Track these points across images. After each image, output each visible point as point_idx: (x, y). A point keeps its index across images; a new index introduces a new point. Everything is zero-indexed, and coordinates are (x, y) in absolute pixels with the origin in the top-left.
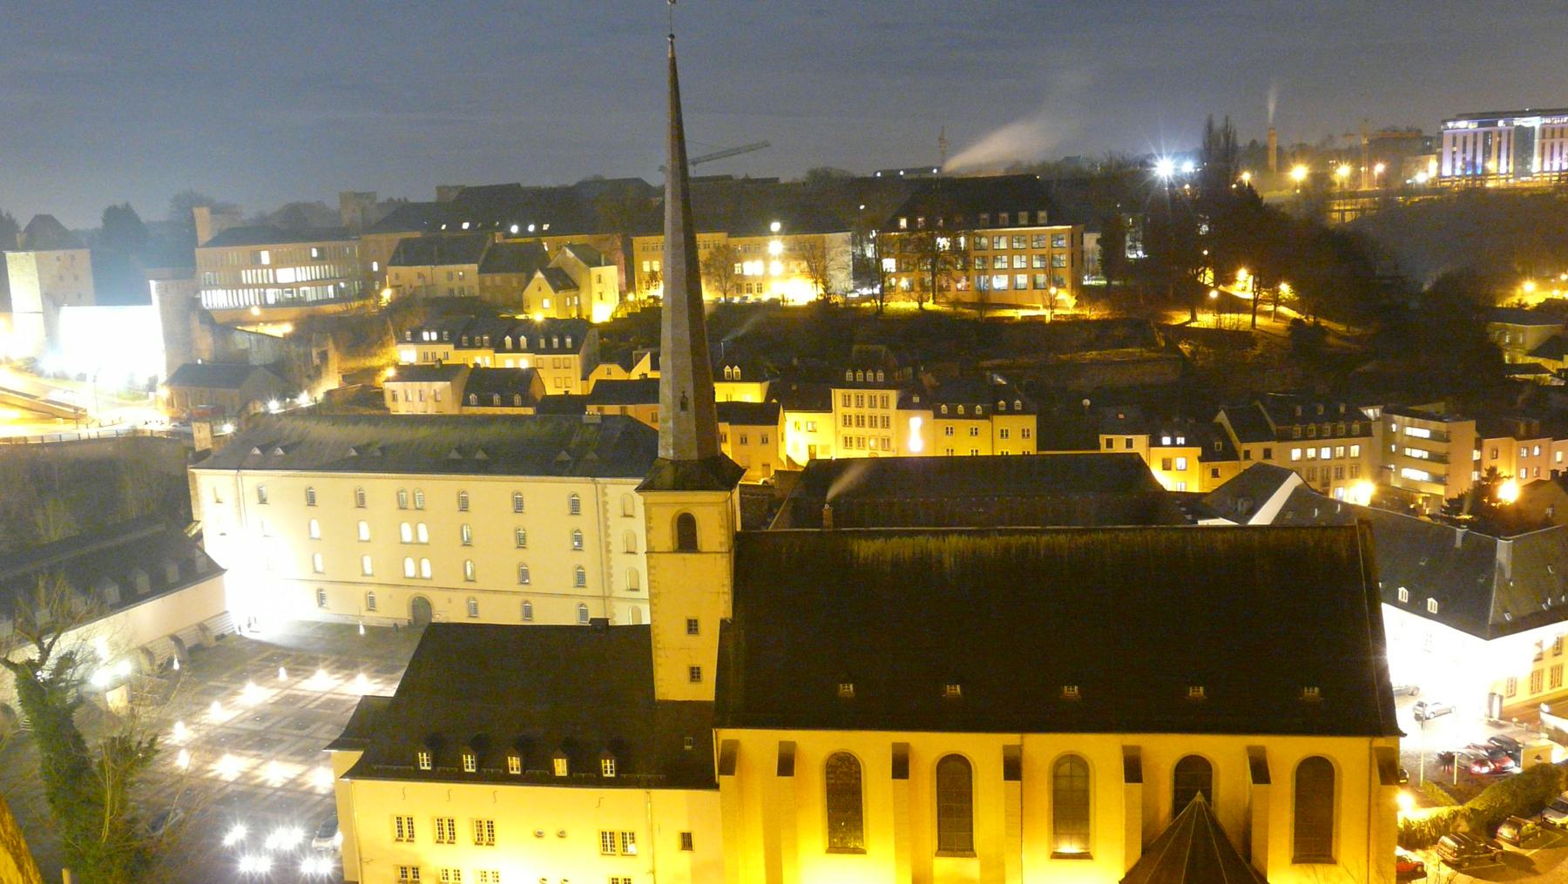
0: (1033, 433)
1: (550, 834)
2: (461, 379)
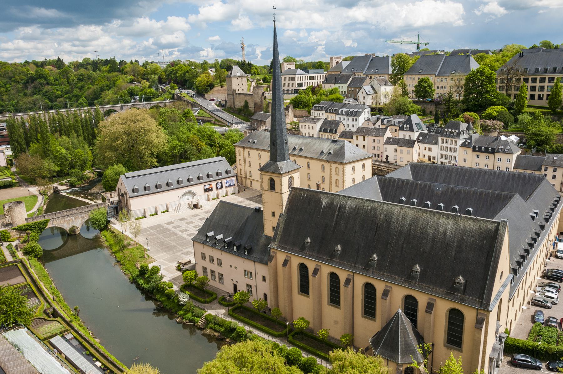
2: (319, 124)
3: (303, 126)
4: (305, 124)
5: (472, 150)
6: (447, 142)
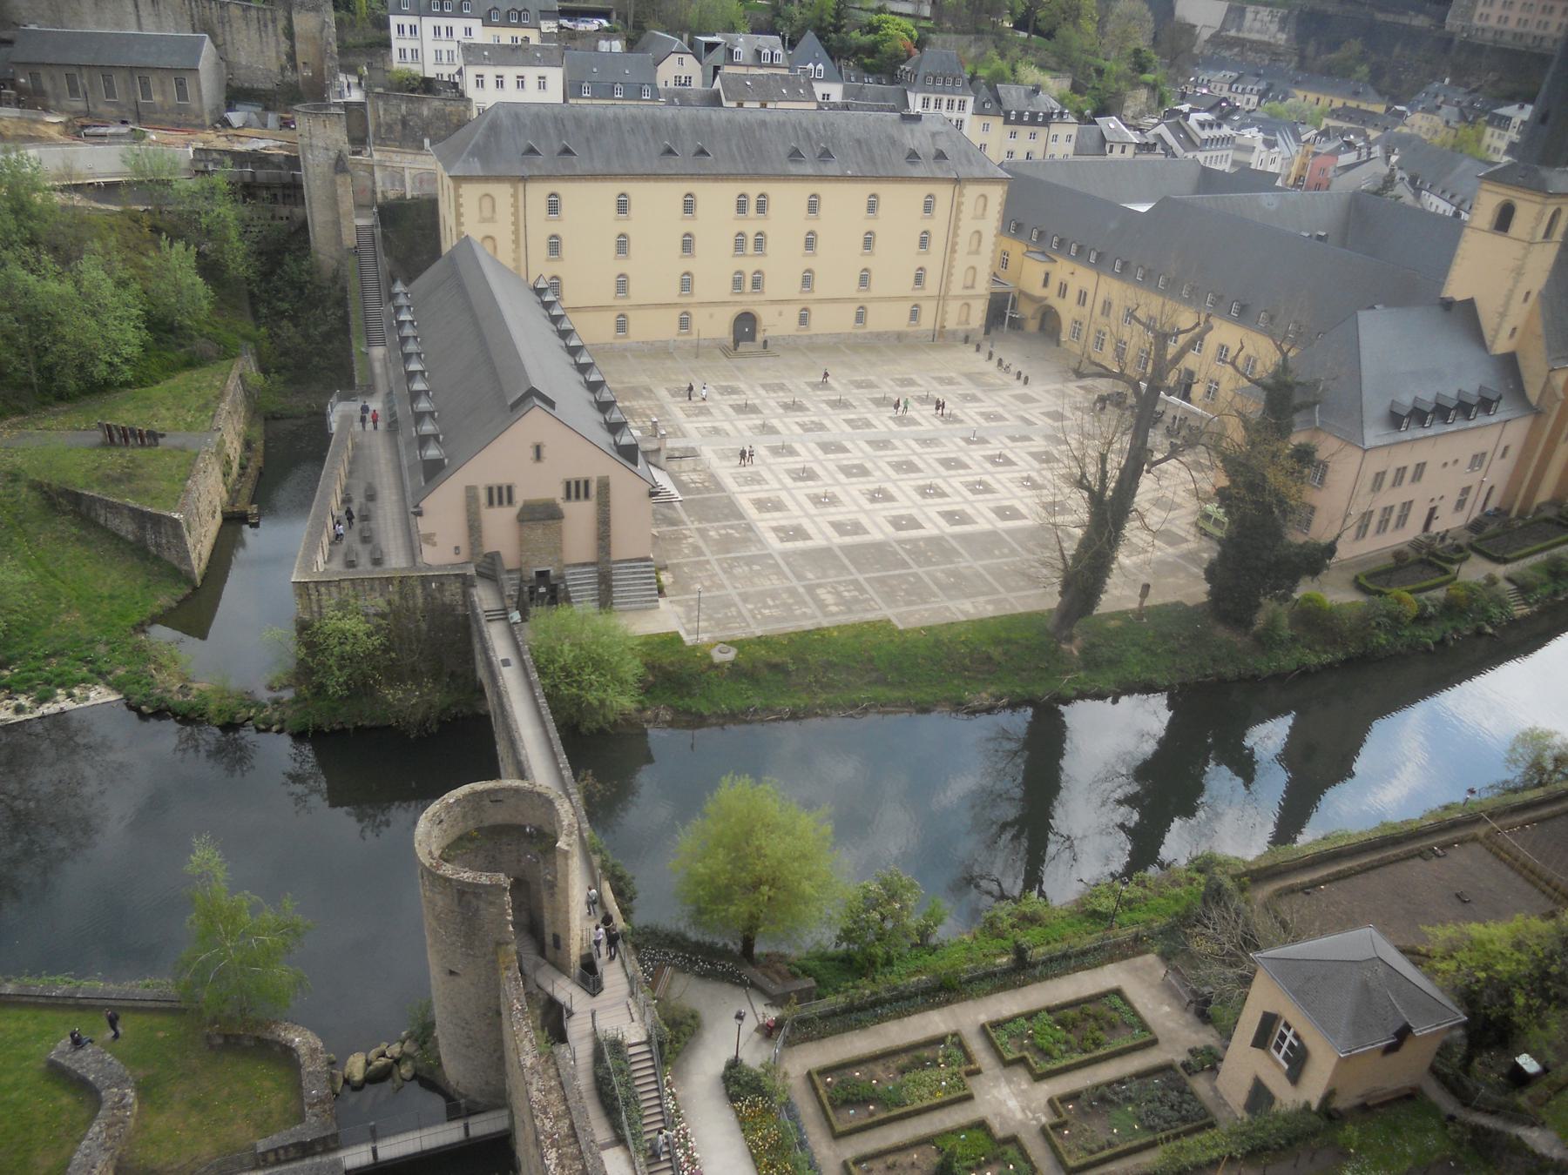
0: (1073, 139)
1: (1450, 461)
3: (490, 81)
4: (500, 70)
5: (1001, 120)
6: (938, 104)
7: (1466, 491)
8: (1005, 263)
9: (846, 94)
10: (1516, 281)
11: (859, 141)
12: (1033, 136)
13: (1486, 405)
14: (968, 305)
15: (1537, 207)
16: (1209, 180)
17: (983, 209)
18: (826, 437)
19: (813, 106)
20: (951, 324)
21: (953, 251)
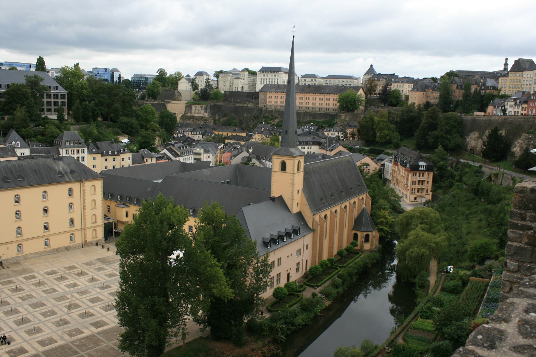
0: (131, 158)
5: (100, 155)
6: (73, 152)
7: (298, 264)
8: (109, 211)
9: (31, 152)
10: (293, 187)
11: (35, 171)
12: (114, 159)
13: (295, 232)
14: (95, 230)
15: (292, 161)
16: (185, 167)
17: (95, 190)
18: (33, 301)
19: (16, 158)
20: (89, 239)
21: (84, 209)
